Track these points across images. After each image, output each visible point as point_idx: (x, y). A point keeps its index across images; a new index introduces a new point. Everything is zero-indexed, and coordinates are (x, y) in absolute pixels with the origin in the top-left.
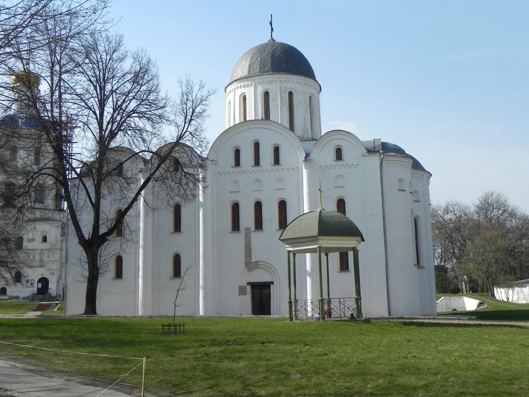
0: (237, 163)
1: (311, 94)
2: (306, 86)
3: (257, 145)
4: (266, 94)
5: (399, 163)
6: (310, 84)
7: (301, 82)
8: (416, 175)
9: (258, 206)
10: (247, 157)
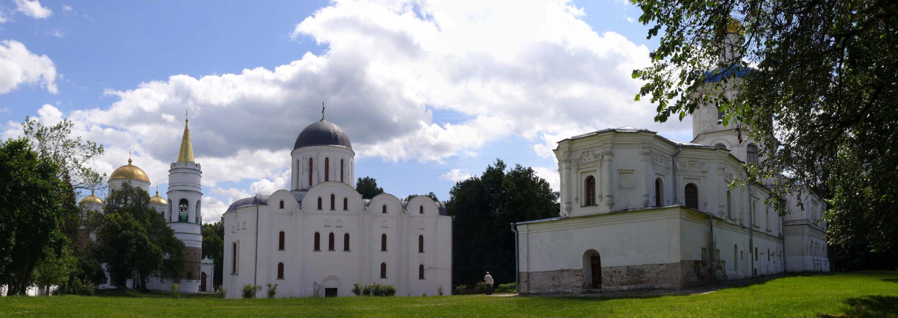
0: (320, 207)
3: (333, 197)
4: (327, 160)
9: (332, 236)
10: (326, 203)
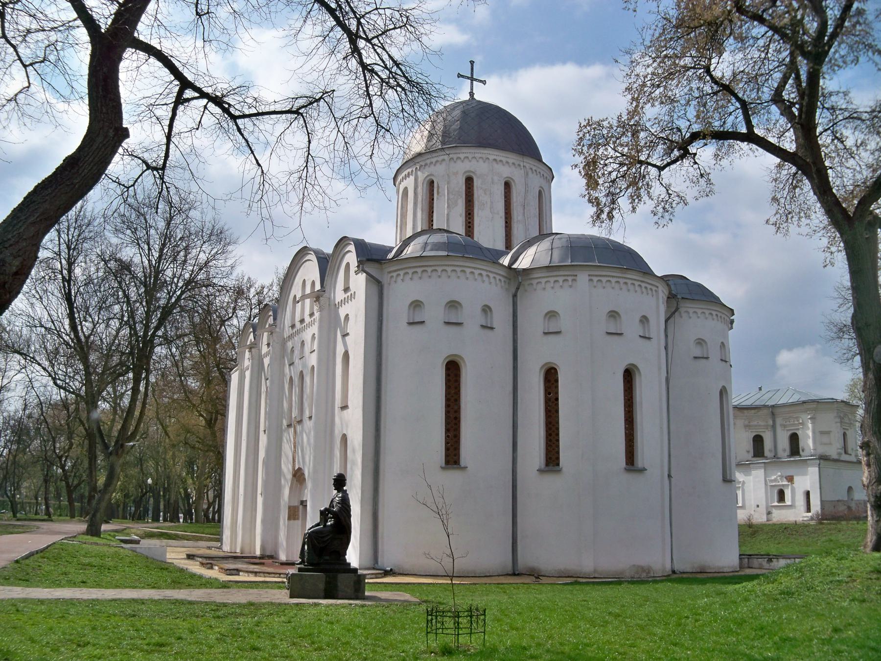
1: (465, 172)
2: (455, 162)
5: (410, 271)
6: (462, 156)
7: (444, 160)
8: (552, 280)
